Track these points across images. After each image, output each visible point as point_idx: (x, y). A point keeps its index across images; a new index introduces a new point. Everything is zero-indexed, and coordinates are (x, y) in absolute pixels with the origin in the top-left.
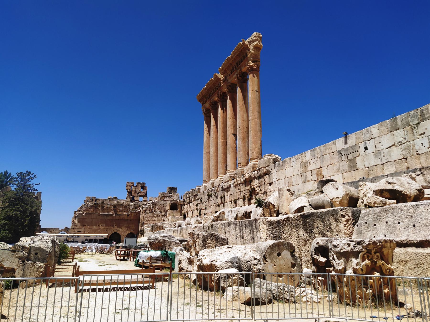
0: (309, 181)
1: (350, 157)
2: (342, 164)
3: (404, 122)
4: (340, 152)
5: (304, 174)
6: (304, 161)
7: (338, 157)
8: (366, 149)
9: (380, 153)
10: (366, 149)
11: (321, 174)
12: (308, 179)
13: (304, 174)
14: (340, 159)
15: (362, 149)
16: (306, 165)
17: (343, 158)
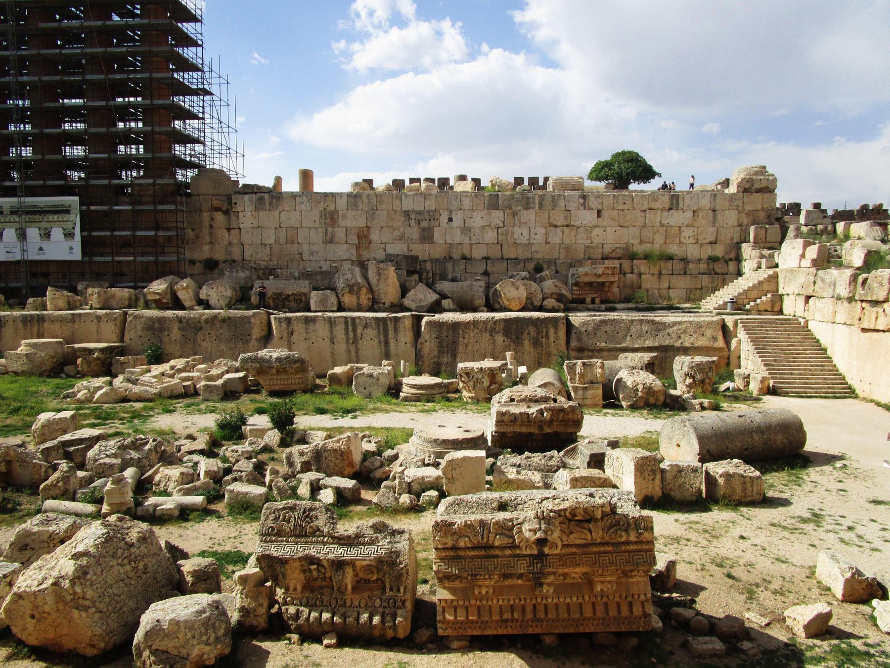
0: (339, 243)
1: (424, 224)
2: (408, 230)
3: (506, 203)
4: (407, 213)
5: (330, 229)
6: (332, 208)
7: (403, 219)
8: (450, 220)
9: (470, 231)
10: (450, 220)
11: (367, 237)
12: (336, 239)
13: (330, 229)
14: (407, 223)
15: (444, 218)
16: (335, 216)
17: (413, 223)
